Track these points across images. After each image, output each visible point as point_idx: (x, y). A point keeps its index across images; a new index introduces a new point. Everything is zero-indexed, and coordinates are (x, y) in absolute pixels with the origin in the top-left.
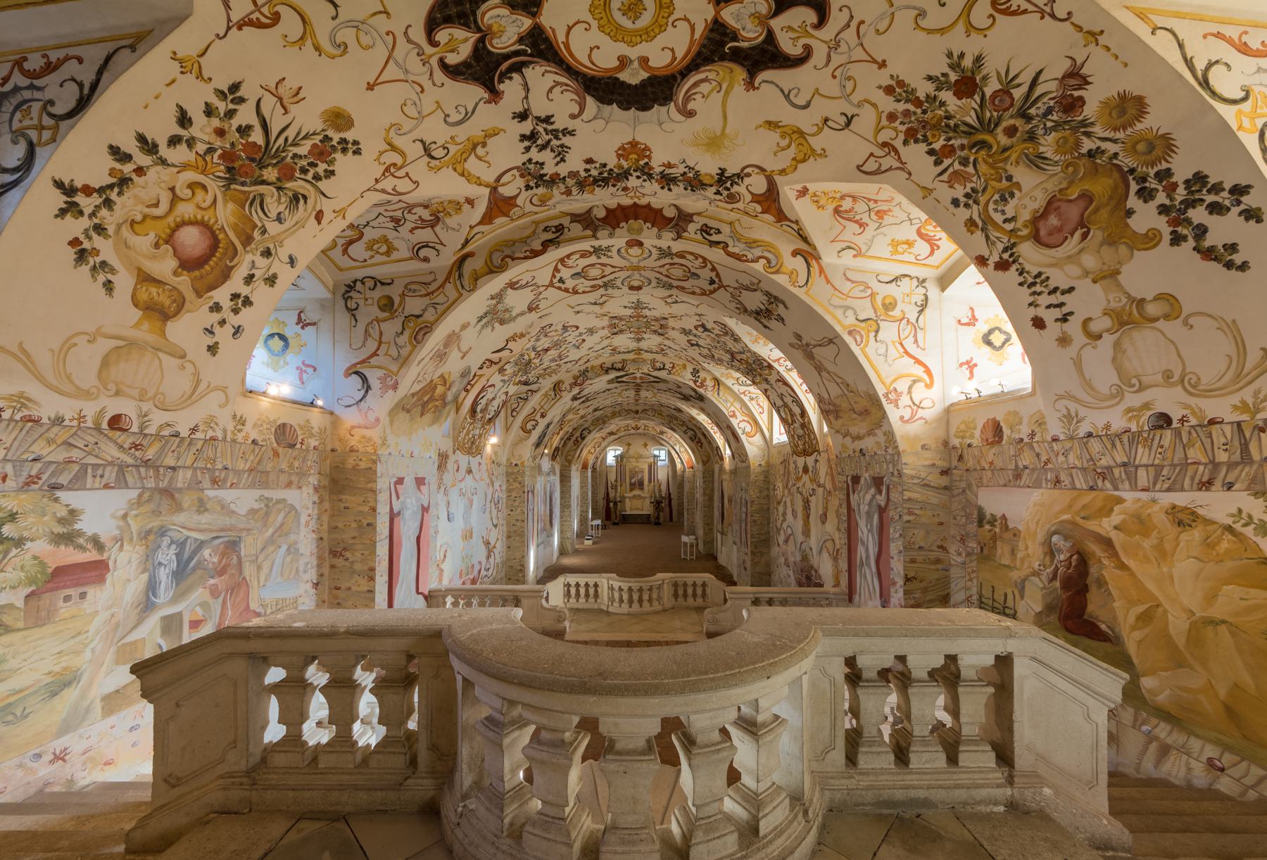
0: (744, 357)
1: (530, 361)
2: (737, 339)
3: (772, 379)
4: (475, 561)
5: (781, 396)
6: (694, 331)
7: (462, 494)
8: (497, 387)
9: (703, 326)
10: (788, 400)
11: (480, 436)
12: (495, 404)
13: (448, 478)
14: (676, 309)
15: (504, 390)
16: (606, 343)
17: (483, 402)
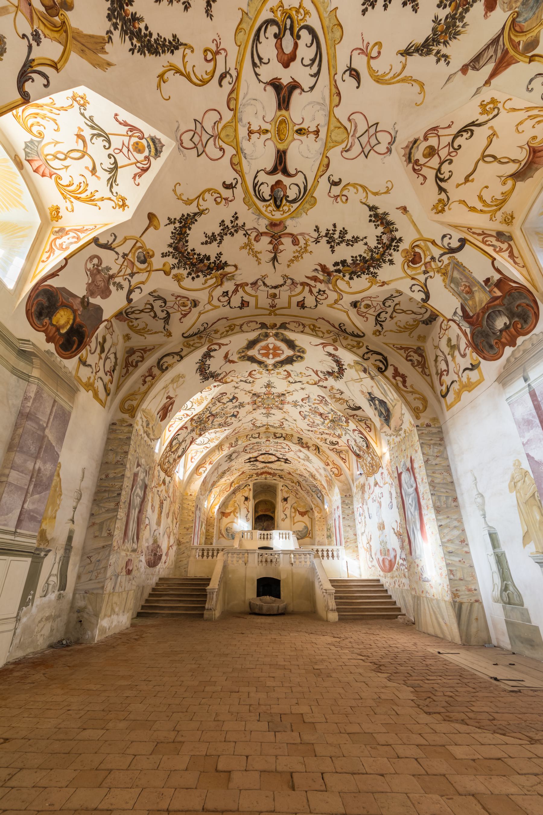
0: (210, 422)
1: (332, 421)
2: (220, 425)
3: (194, 434)
4: (390, 547)
5: (184, 440)
6: (237, 409)
7: (374, 501)
8: (349, 438)
9: (235, 416)
10: (183, 445)
11: (372, 459)
12: (359, 440)
13: (366, 496)
14: (250, 417)
15: (351, 433)
16: (292, 387)
17: (355, 448)
